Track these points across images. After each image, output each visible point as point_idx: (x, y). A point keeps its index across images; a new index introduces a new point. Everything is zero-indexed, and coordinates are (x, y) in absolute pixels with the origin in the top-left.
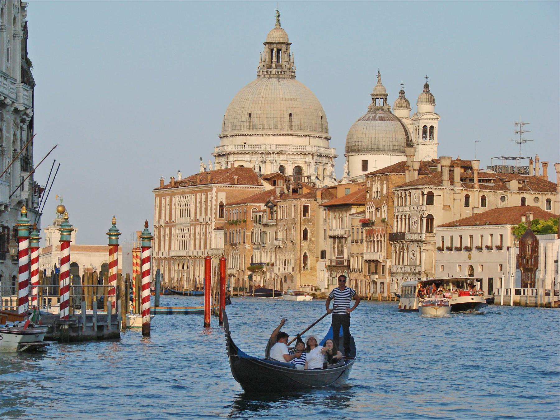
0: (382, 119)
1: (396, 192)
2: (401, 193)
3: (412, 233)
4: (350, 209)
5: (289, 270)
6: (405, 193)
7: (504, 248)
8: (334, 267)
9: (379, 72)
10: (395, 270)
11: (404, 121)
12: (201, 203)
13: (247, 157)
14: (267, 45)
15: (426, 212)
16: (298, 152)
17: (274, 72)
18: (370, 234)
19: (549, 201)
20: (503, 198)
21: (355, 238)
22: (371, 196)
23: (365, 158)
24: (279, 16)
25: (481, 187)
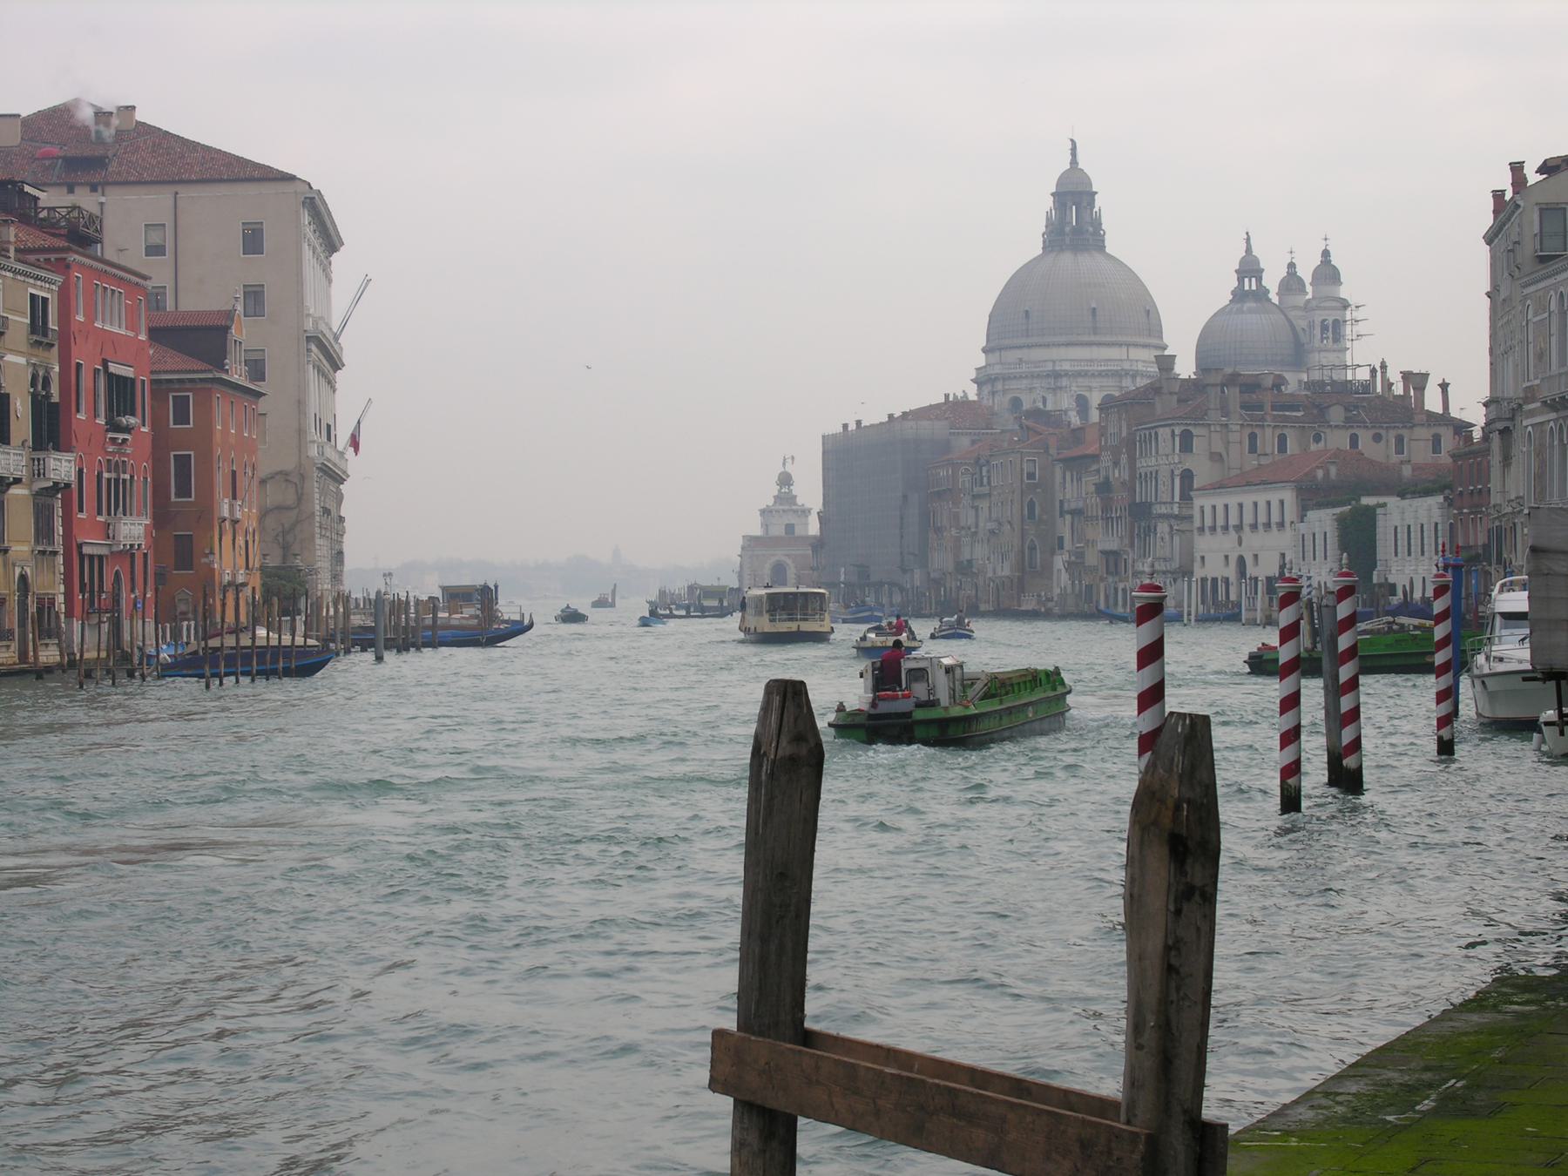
0: (1250, 311)
1: (1138, 433)
2: (1145, 435)
3: (1160, 503)
5: (1006, 572)
7: (1287, 524)
8: (1073, 563)
9: (1247, 233)
10: (1139, 567)
11: (1292, 314)
13: (1024, 383)
15: (1180, 466)
16: (1108, 370)
17: (1068, 242)
20: (1317, 439)
22: (1106, 442)
25: (1275, 418)
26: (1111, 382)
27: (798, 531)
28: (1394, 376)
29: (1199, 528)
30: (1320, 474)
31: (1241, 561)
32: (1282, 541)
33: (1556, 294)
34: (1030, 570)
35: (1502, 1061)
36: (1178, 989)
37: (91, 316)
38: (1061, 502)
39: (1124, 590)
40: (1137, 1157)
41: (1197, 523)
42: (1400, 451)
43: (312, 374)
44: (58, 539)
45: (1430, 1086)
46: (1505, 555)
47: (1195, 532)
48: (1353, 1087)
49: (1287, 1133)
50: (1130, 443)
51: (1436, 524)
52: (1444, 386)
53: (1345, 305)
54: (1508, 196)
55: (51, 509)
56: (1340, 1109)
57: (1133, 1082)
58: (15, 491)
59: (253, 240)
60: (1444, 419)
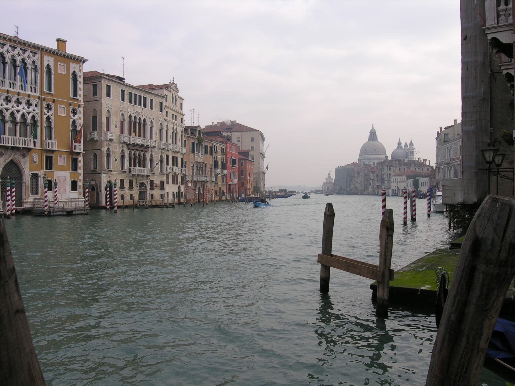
10: (382, 188)
11: (406, 150)
13: (365, 160)
18: (377, 179)
19: (422, 169)
20: (410, 169)
26: (378, 160)
27: (331, 182)
28: (422, 159)
30: (410, 174)
34: (366, 188)
35: (436, 262)
36: (387, 250)
37: (230, 150)
40: (381, 274)
41: (391, 181)
42: (422, 171)
43: (261, 159)
44: (225, 182)
45: (426, 265)
48: (414, 265)
49: (404, 272)
50: (381, 169)
52: (429, 161)
53: (414, 149)
54: (439, 132)
55: (224, 178)
56: (412, 268)
57: (380, 263)
58: (219, 175)
59: (253, 140)
60: (429, 166)
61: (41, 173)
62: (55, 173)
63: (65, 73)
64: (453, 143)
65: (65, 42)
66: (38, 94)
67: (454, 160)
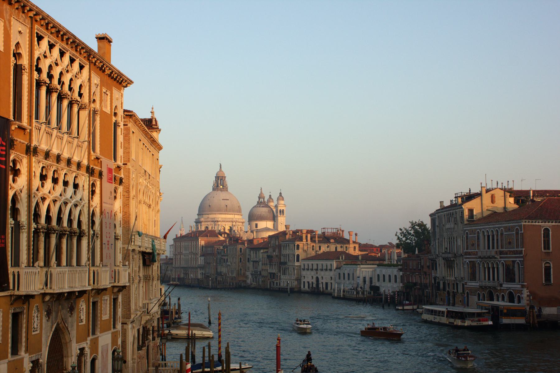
0: (263, 207)
4: (261, 250)
5: (234, 275)
6: (287, 245)
7: (333, 270)
11: (272, 207)
12: (193, 245)
13: (209, 223)
14: (217, 178)
18: (271, 262)
19: (346, 247)
21: (264, 263)
22: (271, 245)
23: (256, 222)
24: (221, 166)
29: (302, 269)
30: (341, 257)
31: (317, 278)
32: (332, 274)
33: (480, 231)
38: (248, 258)
39: (277, 283)
41: (302, 267)
46: (447, 289)
47: (302, 270)
51: (396, 276)
52: (356, 234)
61: (86, 345)
62: (100, 339)
63: (108, 110)
64: (501, 227)
65: (110, 42)
66: (85, 162)
67: (501, 253)
